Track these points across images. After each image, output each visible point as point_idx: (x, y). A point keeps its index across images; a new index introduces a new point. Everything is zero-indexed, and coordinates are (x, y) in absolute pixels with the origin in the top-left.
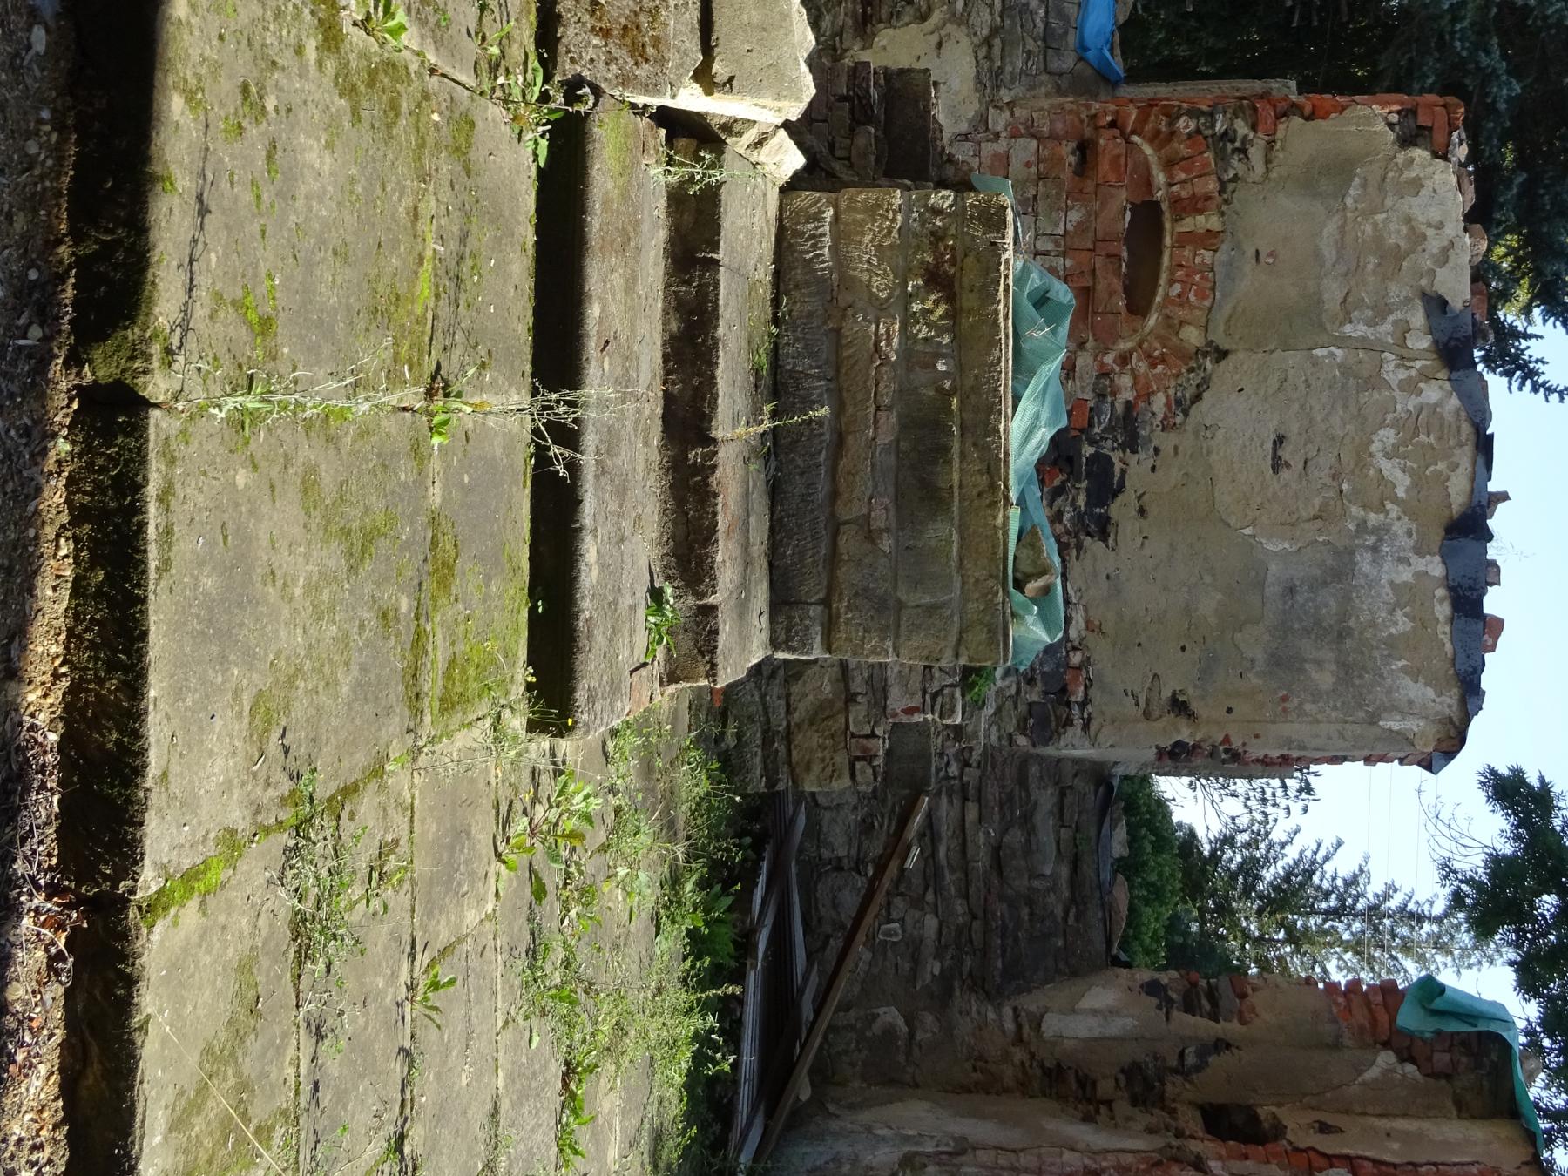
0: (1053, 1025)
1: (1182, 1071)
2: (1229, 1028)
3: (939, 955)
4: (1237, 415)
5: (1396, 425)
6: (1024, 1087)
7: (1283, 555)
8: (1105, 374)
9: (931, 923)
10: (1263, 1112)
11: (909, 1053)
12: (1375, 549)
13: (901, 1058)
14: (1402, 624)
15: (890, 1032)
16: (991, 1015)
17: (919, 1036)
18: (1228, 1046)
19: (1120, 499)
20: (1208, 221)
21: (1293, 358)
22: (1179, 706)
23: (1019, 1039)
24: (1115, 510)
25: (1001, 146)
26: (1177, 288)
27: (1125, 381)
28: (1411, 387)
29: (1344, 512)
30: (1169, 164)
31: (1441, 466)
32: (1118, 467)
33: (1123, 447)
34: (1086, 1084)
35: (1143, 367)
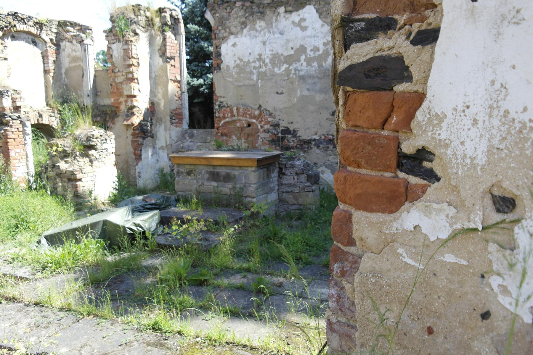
4: (273, 103)
5: (273, 68)
7: (301, 91)
12: (299, 71)
14: (315, 64)
19: (290, 128)
20: (235, 109)
21: (260, 91)
24: (291, 129)
26: (248, 116)
28: (266, 65)
29: (292, 78)
30: (224, 117)
31: (282, 57)
32: (283, 128)
33: (279, 127)
35: (263, 123)
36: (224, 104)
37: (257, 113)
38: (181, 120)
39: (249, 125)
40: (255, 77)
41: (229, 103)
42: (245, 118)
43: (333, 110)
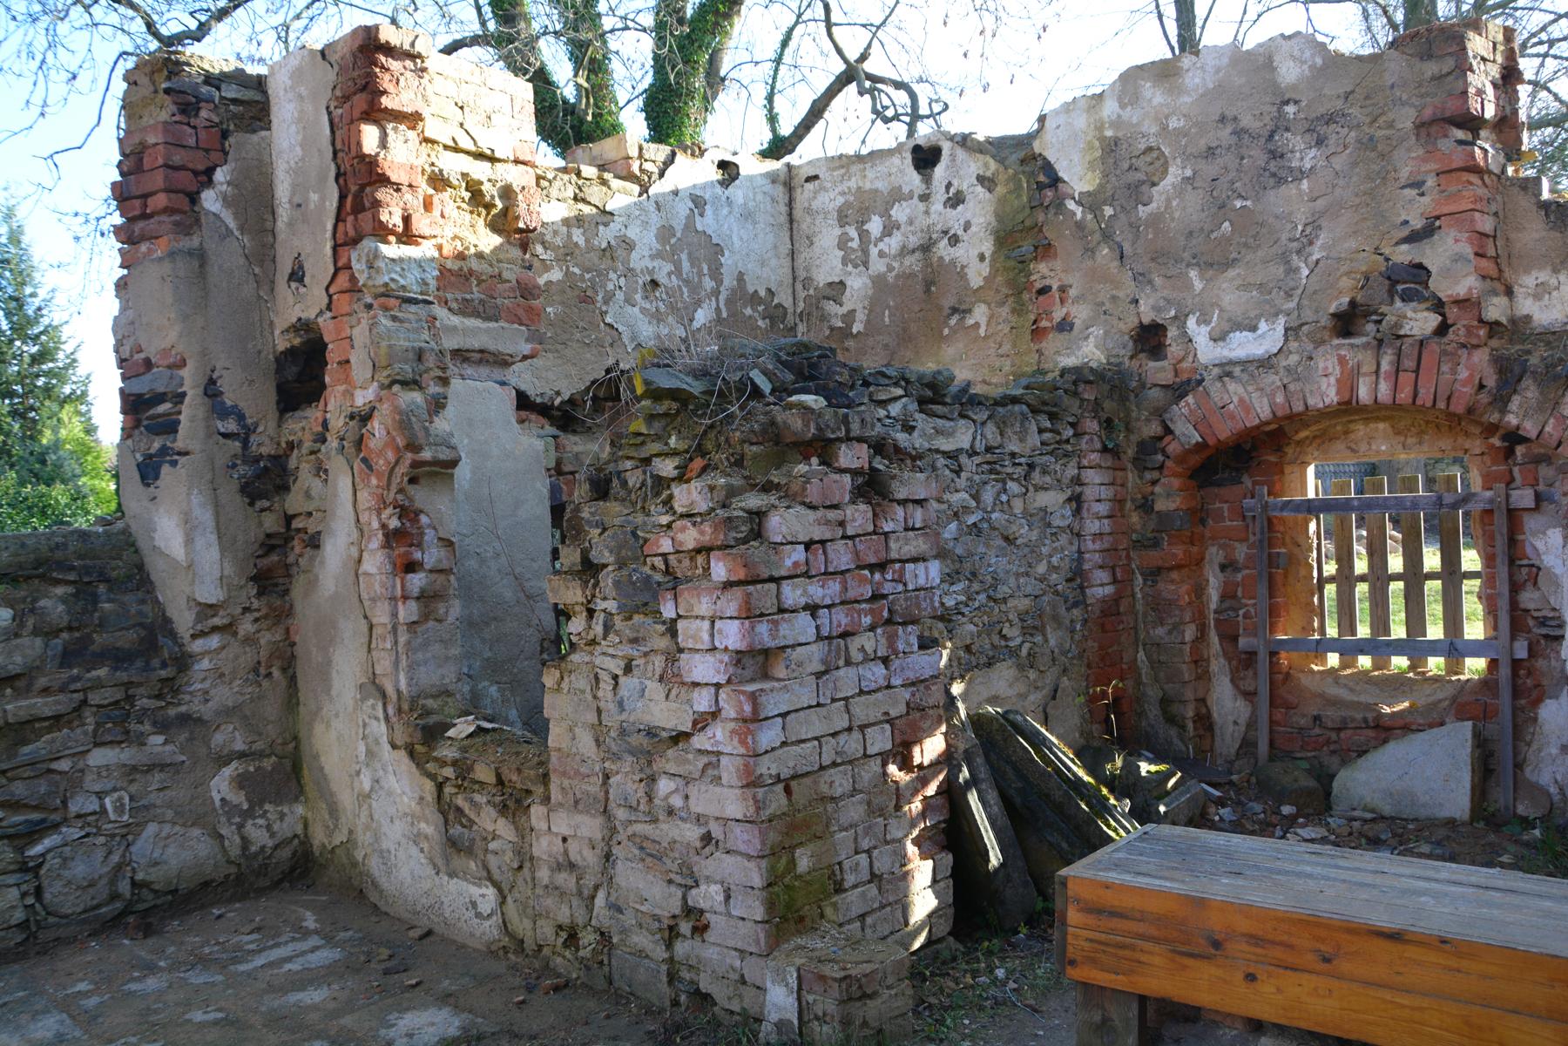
0: (210, 593)
1: (244, 436)
2: (190, 380)
6: (281, 615)
10: (282, 345)
11: (261, 755)
13: (268, 764)
15: (241, 782)
16: (205, 664)
17: (239, 746)
18: (212, 382)
23: (228, 629)
34: (275, 544)
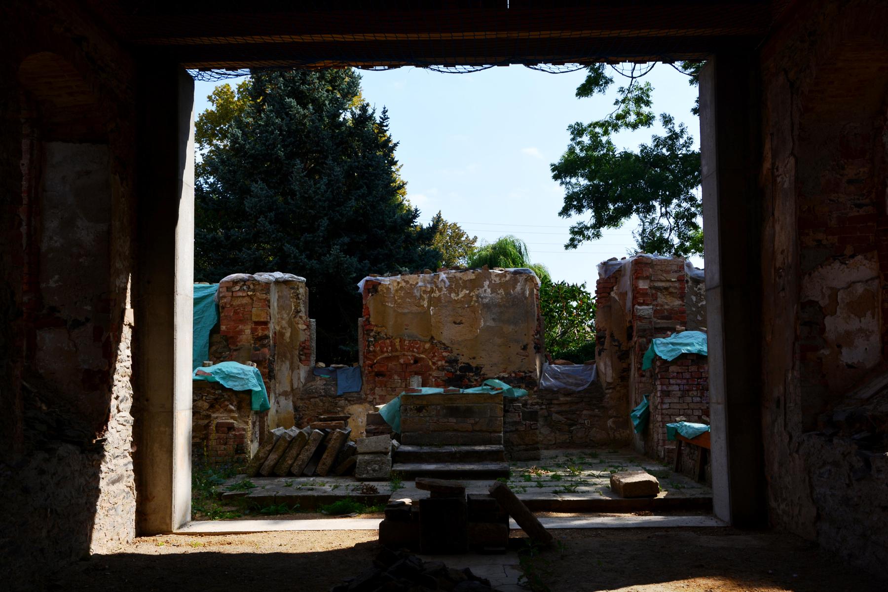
0: (609, 380)
1: (619, 346)
3: (593, 410)
4: (448, 333)
8: (438, 368)
9: (585, 412)
12: (482, 298)
13: (621, 419)
14: (501, 291)
15: (614, 422)
21: (433, 320)
22: (525, 348)
23: (614, 388)
24: (474, 365)
25: (377, 397)
27: (440, 363)
30: (382, 352)
35: (436, 359)
36: (382, 335)
37: (427, 346)
38: (308, 356)
39: (417, 361)
40: (425, 304)
41: (390, 333)
42: (410, 353)
43: (525, 343)
